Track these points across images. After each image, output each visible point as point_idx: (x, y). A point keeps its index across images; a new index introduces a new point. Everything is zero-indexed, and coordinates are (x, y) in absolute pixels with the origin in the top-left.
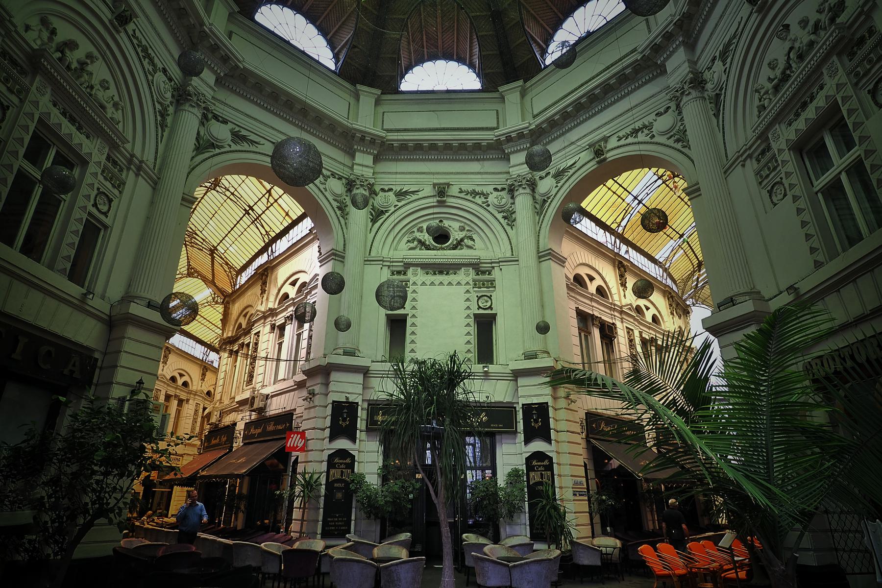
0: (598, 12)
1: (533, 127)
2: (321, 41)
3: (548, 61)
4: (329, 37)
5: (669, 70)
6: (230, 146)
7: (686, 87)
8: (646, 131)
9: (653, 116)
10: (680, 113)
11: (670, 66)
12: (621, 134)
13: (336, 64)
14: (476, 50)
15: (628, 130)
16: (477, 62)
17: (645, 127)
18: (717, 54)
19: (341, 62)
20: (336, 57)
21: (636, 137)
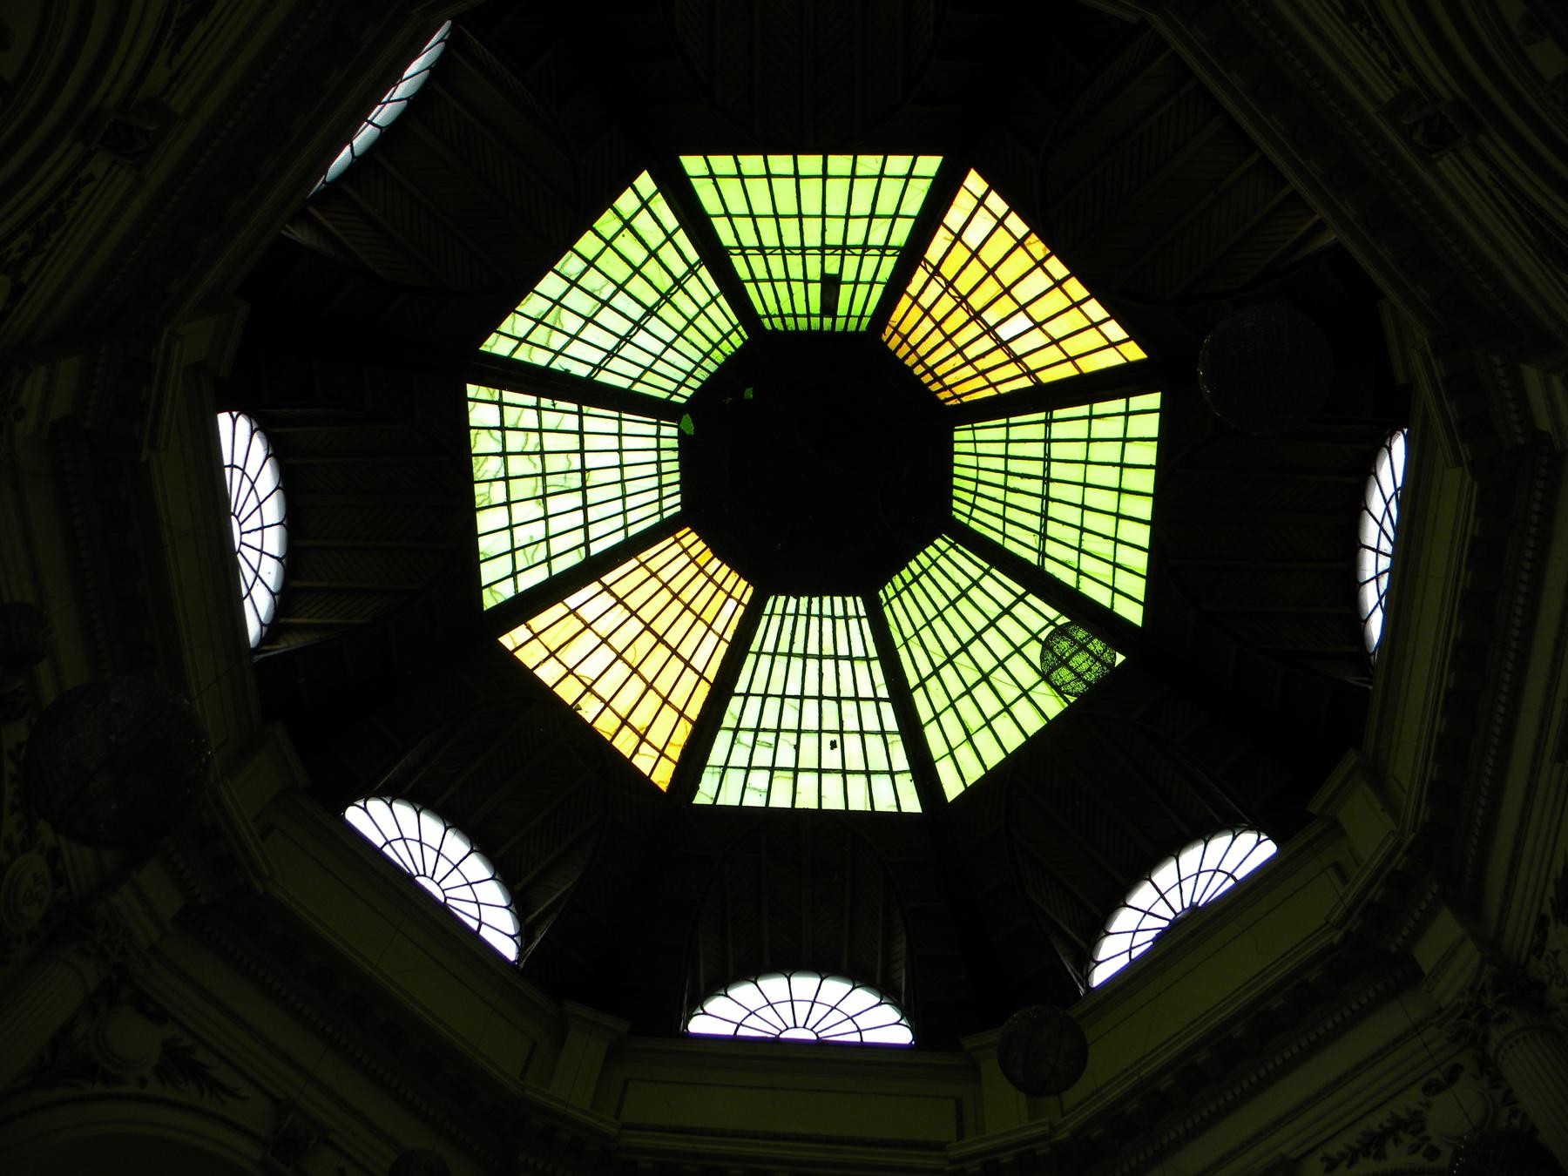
0: (1210, 864)
1: (1063, 1135)
2: (493, 893)
3: (1100, 976)
4: (518, 887)
5: (1426, 965)
6: (143, 1082)
7: (1488, 1001)
8: (1408, 1139)
9: (1414, 1097)
10: (1497, 1080)
11: (1427, 954)
12: (1334, 1149)
13: (521, 950)
14: (901, 947)
15: (1352, 1138)
16: (902, 976)
17: (1399, 1125)
18: (1547, 909)
19: (535, 945)
20: (524, 935)
21: (1380, 1156)
